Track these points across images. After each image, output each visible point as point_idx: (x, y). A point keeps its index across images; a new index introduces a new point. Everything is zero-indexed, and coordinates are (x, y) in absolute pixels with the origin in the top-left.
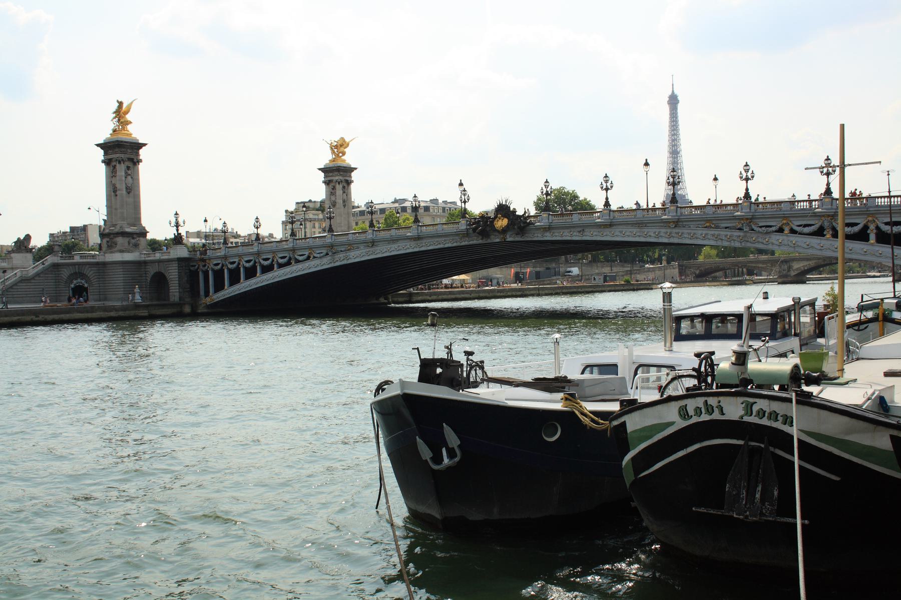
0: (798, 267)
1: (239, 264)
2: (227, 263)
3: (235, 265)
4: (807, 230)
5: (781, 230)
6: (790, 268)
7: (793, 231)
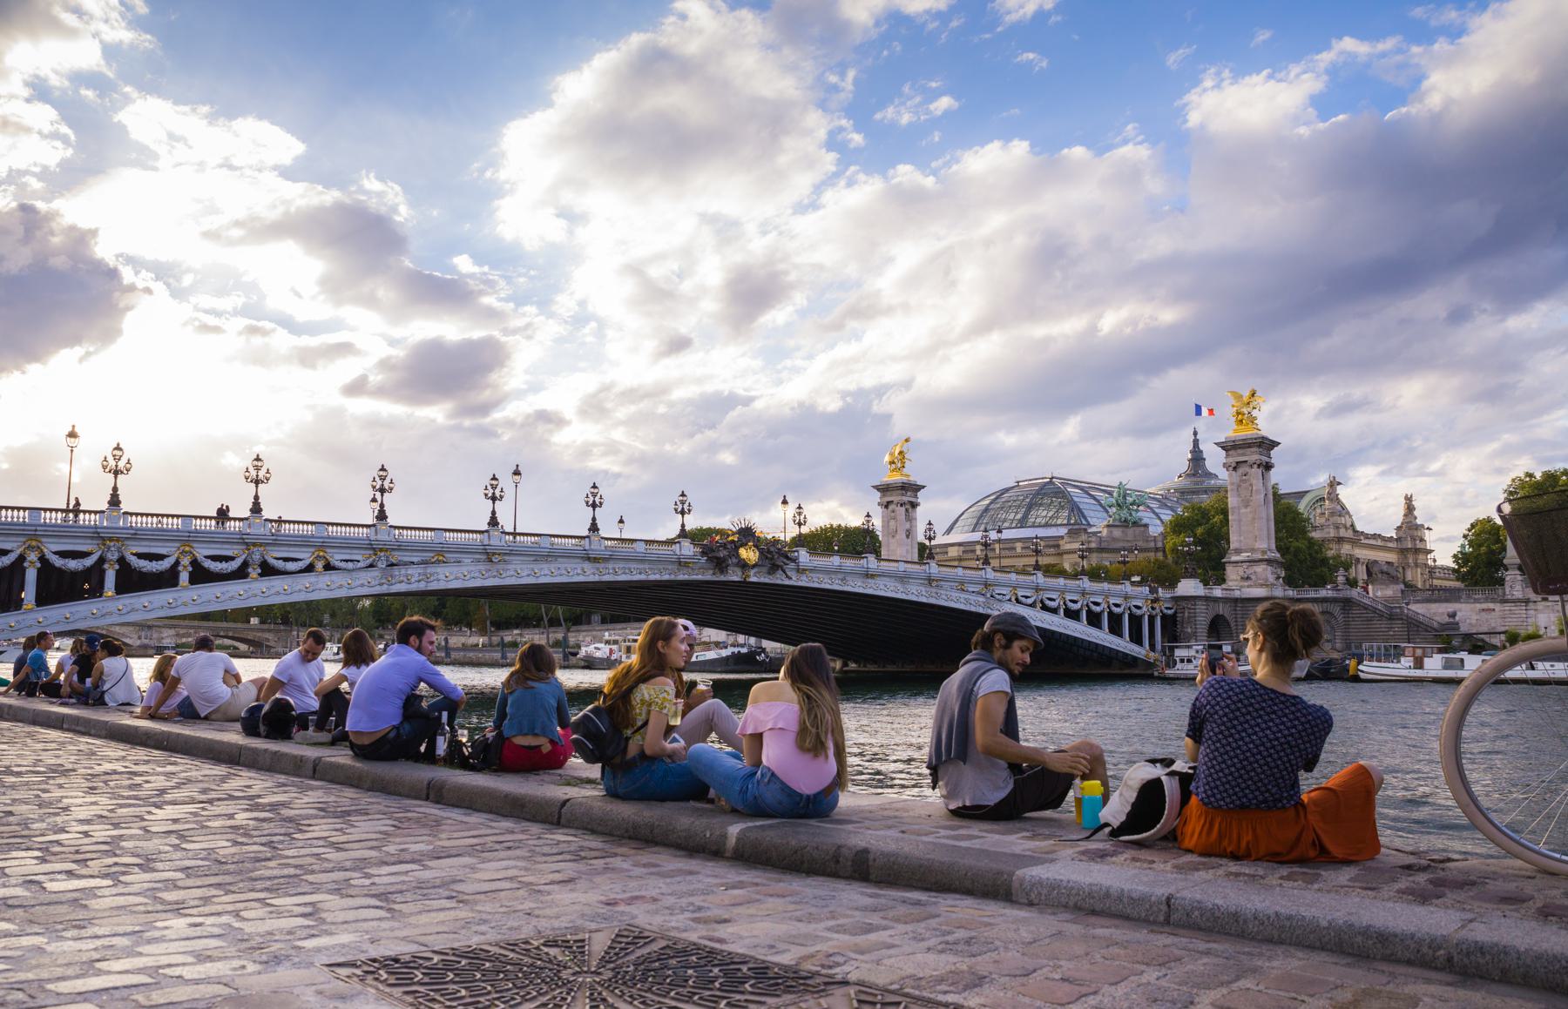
1: (22, 558)
5: (1010, 600)
7: (1018, 601)
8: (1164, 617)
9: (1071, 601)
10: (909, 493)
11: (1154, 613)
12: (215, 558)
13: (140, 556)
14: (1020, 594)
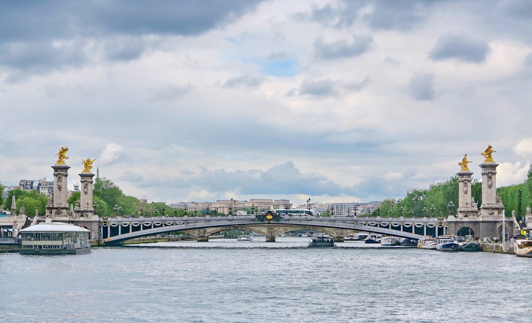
0: (210, 231)
1: (129, 225)
2: (122, 224)
3: (127, 225)
4: (373, 225)
5: (365, 225)
6: (205, 231)
7: (368, 225)
8: (446, 228)
9: (394, 224)
10: (465, 177)
11: (440, 227)
12: (157, 223)
13: (146, 224)
14: (369, 223)
